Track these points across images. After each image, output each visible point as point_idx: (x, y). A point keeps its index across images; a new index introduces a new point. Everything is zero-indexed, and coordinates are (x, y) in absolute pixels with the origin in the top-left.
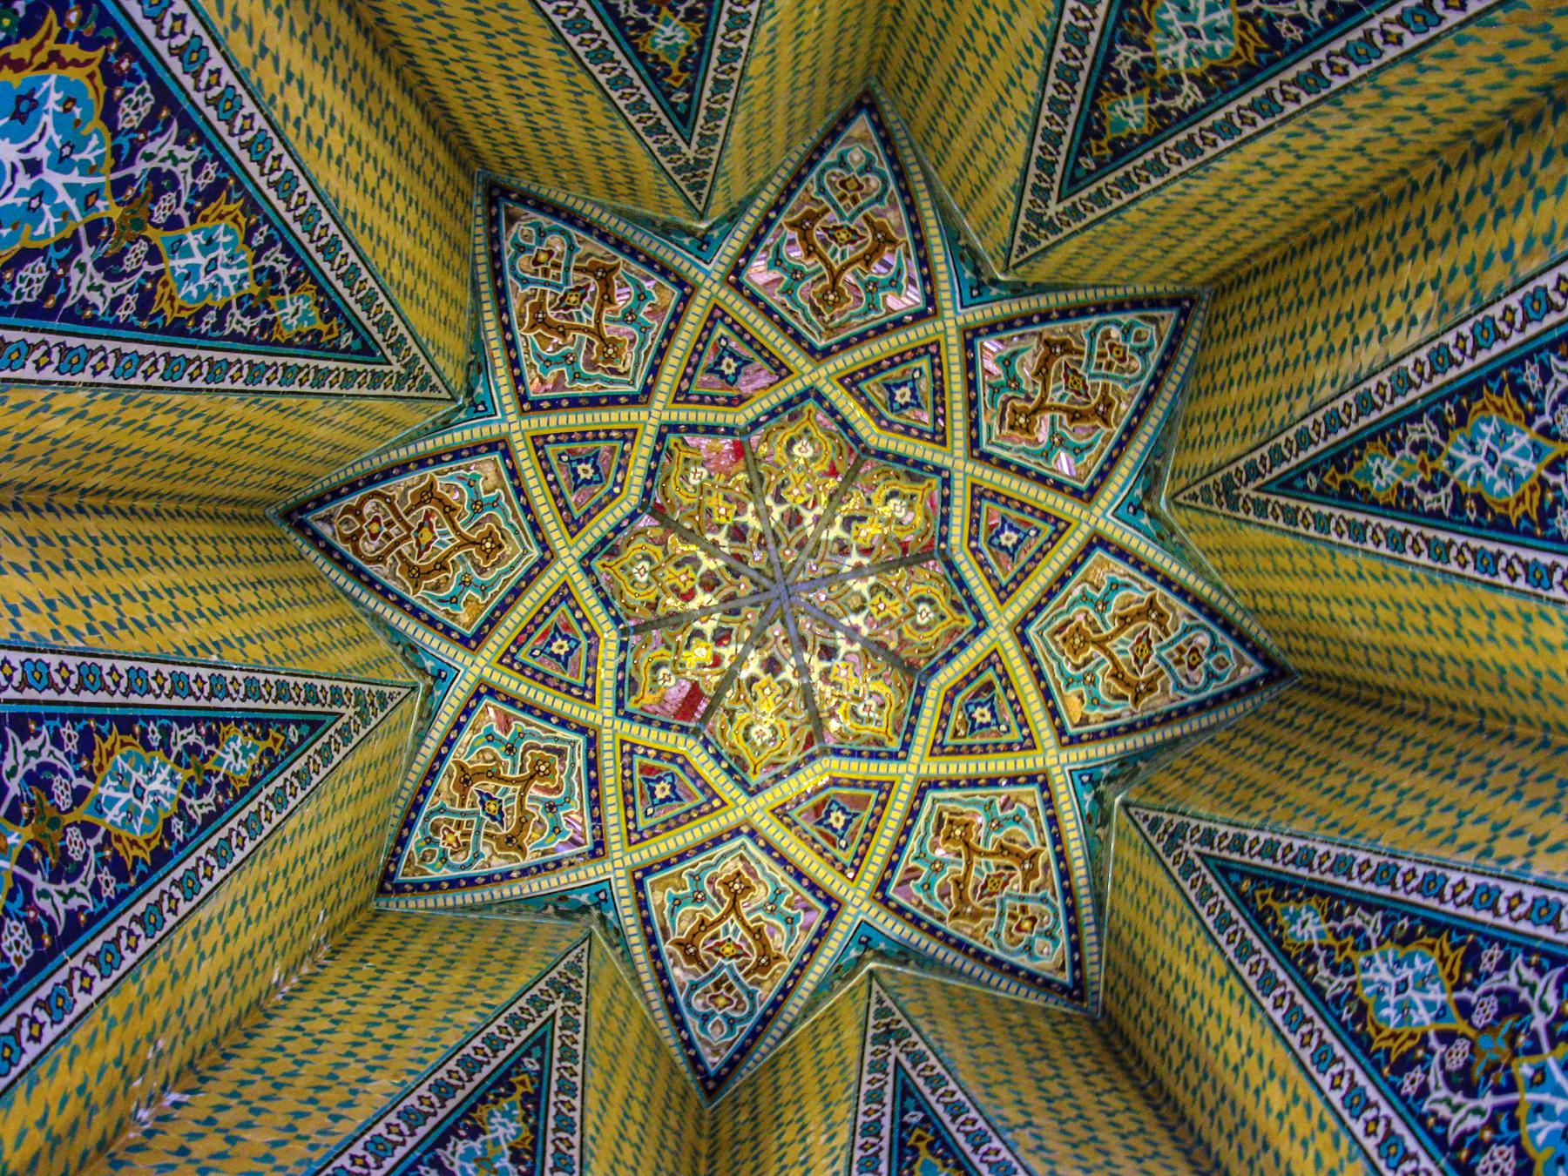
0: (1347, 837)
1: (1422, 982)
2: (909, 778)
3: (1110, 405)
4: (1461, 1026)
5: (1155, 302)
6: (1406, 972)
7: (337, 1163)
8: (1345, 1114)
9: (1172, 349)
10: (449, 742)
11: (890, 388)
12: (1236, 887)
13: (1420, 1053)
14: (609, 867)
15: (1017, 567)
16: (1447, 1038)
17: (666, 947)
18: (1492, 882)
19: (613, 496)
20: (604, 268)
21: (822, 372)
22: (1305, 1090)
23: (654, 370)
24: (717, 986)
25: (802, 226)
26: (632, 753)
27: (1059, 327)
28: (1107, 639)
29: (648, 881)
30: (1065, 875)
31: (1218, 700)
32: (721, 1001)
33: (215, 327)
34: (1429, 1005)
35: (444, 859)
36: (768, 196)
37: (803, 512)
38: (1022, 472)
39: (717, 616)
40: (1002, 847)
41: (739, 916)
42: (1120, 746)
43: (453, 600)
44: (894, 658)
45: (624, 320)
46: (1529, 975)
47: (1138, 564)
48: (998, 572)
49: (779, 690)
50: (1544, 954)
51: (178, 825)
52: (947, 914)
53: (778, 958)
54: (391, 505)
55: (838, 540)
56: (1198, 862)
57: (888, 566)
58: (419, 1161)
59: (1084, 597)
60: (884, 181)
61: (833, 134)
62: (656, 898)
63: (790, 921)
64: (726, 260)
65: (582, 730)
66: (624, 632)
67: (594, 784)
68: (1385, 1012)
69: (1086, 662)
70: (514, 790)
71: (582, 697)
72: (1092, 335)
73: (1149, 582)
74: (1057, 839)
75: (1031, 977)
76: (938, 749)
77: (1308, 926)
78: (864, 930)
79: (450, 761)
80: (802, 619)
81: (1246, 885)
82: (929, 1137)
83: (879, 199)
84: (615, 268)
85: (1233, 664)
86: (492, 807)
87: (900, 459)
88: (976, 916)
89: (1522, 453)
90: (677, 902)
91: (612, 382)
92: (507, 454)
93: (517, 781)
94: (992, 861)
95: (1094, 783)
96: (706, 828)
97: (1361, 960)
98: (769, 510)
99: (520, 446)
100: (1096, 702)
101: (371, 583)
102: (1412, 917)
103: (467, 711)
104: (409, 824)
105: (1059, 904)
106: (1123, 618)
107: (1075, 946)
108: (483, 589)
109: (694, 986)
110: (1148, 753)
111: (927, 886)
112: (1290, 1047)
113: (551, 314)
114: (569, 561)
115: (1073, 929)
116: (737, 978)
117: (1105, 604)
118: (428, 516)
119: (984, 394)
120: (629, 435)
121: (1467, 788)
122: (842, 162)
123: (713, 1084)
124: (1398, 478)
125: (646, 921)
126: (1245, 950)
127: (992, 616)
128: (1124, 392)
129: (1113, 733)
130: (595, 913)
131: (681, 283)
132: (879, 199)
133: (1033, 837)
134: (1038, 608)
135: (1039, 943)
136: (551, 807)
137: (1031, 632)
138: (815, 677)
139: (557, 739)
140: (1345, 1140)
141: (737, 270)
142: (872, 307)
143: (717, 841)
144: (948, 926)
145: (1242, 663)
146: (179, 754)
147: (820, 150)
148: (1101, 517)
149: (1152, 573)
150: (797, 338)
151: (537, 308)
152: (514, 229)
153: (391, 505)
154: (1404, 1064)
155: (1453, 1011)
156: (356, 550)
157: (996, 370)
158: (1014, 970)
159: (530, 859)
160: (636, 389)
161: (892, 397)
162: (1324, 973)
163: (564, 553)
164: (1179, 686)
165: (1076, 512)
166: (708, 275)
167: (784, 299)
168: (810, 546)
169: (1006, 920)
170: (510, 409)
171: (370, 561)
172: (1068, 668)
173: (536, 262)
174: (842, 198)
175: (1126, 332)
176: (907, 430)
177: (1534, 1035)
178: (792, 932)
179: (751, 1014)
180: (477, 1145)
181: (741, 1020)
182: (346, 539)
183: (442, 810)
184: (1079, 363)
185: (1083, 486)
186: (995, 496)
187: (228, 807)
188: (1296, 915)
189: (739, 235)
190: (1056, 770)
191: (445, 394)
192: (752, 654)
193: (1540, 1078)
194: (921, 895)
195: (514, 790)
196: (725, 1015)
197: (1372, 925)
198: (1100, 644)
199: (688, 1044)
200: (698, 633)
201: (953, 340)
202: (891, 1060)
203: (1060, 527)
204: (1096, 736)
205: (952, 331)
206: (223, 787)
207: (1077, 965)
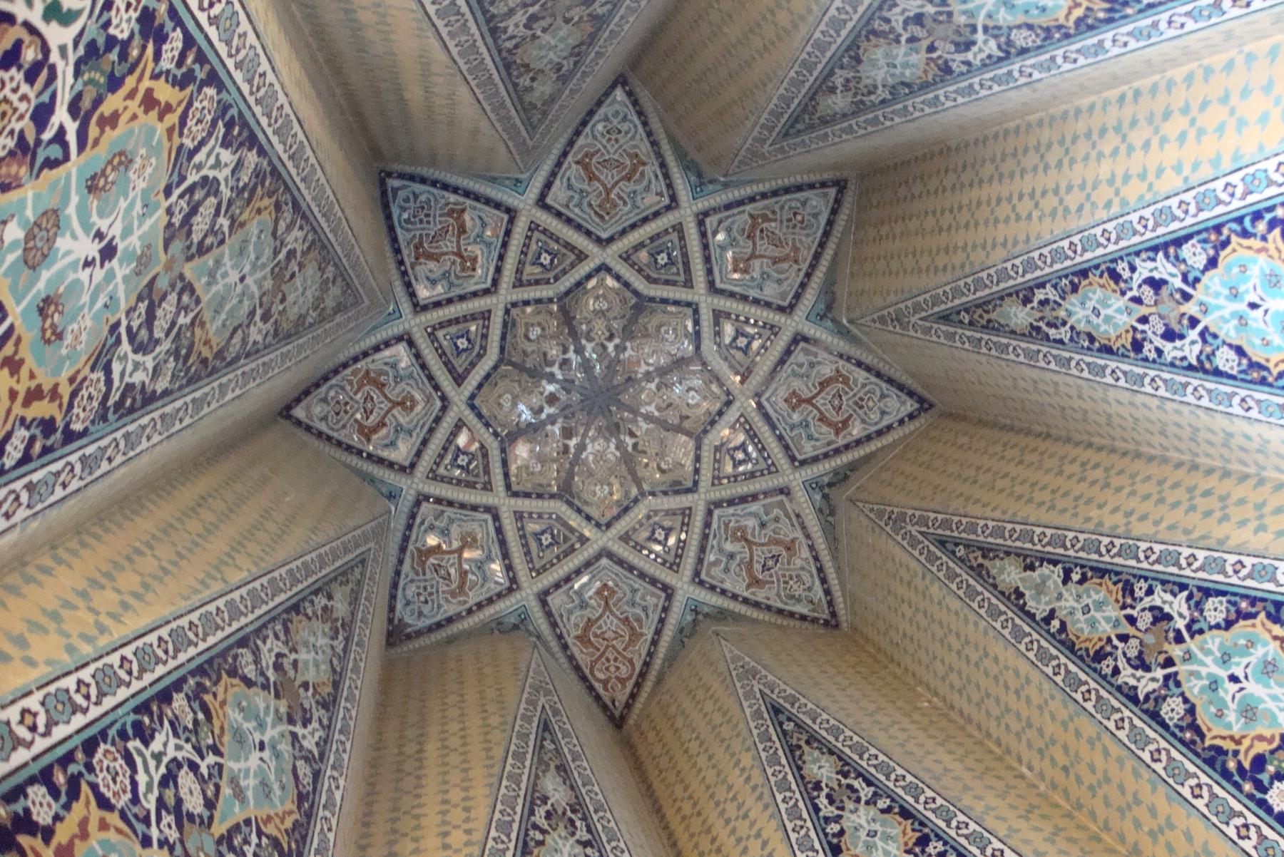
2: (709, 300)
3: (453, 211)
5: (384, 193)
7: (1061, 684)
9: (412, 178)
10: (735, 597)
11: (459, 352)
12: (799, 131)
13: (940, 62)
14: (794, 483)
15: (564, 251)
17: (841, 442)
19: (559, 519)
20: (419, 558)
21: (456, 399)
23: (475, 508)
24: (861, 407)
25: (367, 433)
26: (719, 478)
27: (405, 252)
28: (604, 185)
29: (799, 457)
30: (764, 196)
31: (640, 114)
32: (871, 404)
33: (592, 847)
35: (809, 589)
36: (354, 460)
37: (546, 394)
38: (501, 258)
39: (622, 437)
40: (748, 237)
41: (814, 397)
42: (675, 170)
43: (645, 609)
44: (633, 320)
45: (448, 535)
47: (553, 174)
48: (568, 262)
49: (664, 390)
51: (883, 803)
52: (796, 267)
53: (838, 371)
54: (596, 662)
55: (560, 368)
57: (574, 334)
58: (1048, 632)
59: (579, 205)
60: (331, 387)
61: (308, 429)
62: (808, 450)
63: (812, 365)
64: (398, 478)
65: (710, 513)
66: (643, 494)
67: (743, 499)
69: (620, 198)
70: (757, 551)
71: (690, 516)
72: (408, 230)
73: (565, 166)
74: (740, 203)
75: (834, 212)
76: (689, 284)
78: (812, 317)
79: (746, 594)
80: (615, 382)
81: (800, 126)
82: (980, 311)
83: (343, 388)
84: (418, 549)
85: (617, 107)
86: (770, 563)
87: (503, 337)
88: (796, 250)
90: (810, 437)
91: (488, 534)
92: (546, 593)
93: (750, 549)
94: (759, 243)
95: (701, 184)
96: (760, 424)
98: (549, 416)
99: (540, 585)
100: (647, 189)
101: (647, 664)
103: (713, 588)
104: (792, 615)
105: (784, 198)
106: (590, 179)
107: (811, 186)
108: (634, 591)
109: (863, 421)
110: (681, 155)
113: (454, 586)
114: (605, 539)
115: (799, 188)
116: (855, 395)
117: (582, 191)
118: (596, 636)
119: (457, 292)
120: (519, 516)
122: (325, 418)
123: (924, 405)
125: (826, 456)
126: (849, 130)
127: (597, 262)
128: (443, 201)
129: (667, 176)
130: (826, 490)
131: (418, 503)
132: (343, 388)
133: (741, 218)
134: (588, 233)
135: (808, 210)
136: (763, 525)
137: (604, 235)
138: (651, 369)
139: (719, 527)
141: (403, 469)
142: (411, 376)
143: (766, 417)
144: (805, 267)
145: (614, 101)
146: (838, 808)
147: (320, 434)
148: (525, 202)
149: (559, 164)
150: (438, 420)
151: (453, 594)
152: (410, 622)
153: (596, 662)
156: (629, 678)
157: (439, 289)
158: (830, 223)
159: (799, 534)
160: (488, 517)
161: (465, 350)
162: (873, 97)
163: (601, 543)
164: (633, 138)
165: (523, 219)
166: (410, 487)
167: (414, 434)
168: (566, 385)
169: (797, 230)
170: (518, 596)
171: (634, 669)
172: (627, 209)
173: (426, 602)
174: (346, 412)
175: (403, 209)
176: (485, 336)
178: (819, 363)
179: (877, 385)
180: (1027, 593)
181: (881, 389)
182: (624, 686)
183: (778, 595)
184: (427, 235)
185: (506, 217)
186: (519, 271)
187: (855, 769)
188: (828, 106)
189: (381, 473)
190: (694, 208)
191: (536, 655)
192: (643, 410)
195: (757, 551)
198: (608, 192)
199: (901, 422)
200: (635, 446)
201: (423, 318)
202: (920, 323)
203: (533, 227)
204: (670, 186)
205: (418, 320)
206: (846, 775)
207: (824, 185)
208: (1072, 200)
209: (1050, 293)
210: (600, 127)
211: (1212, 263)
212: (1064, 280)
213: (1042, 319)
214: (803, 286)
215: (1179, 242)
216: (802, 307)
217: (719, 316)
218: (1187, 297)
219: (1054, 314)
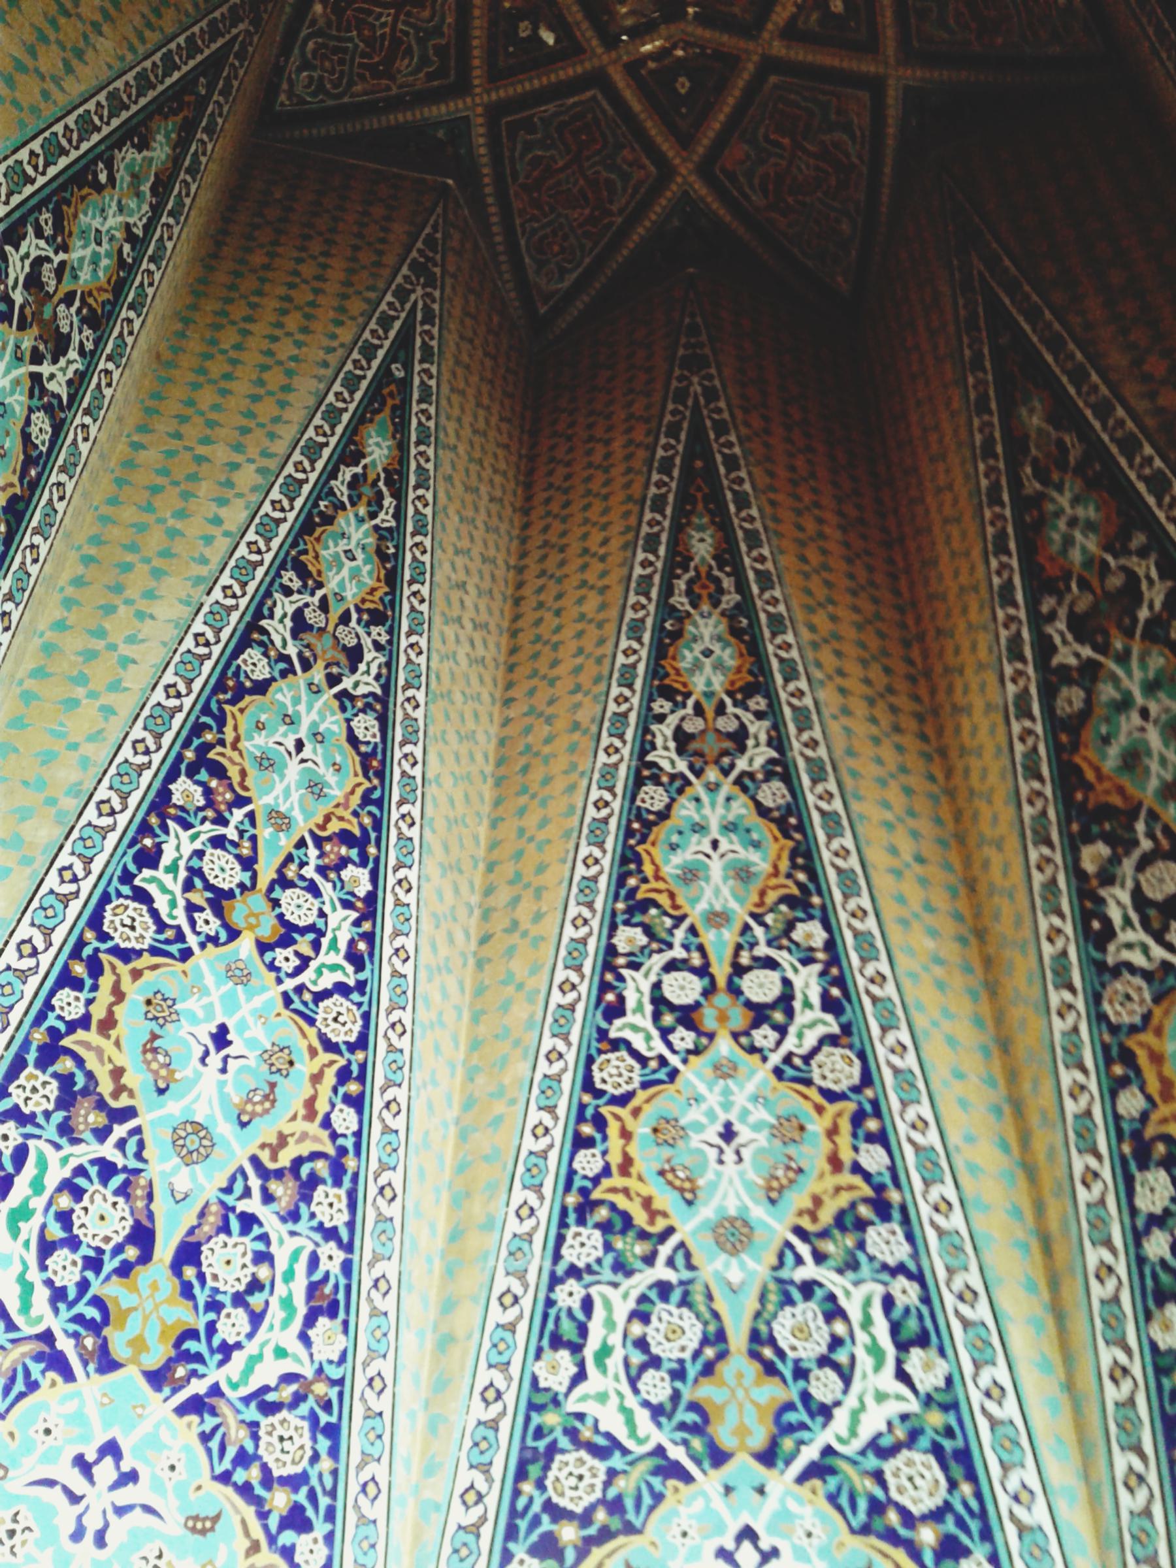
0: (771, 524)
1: (718, 666)
4: (710, 712)
6: (716, 648)
8: (616, 675)
16: (699, 710)
18: (801, 668)
22: (611, 628)
24: (336, 51)
34: (709, 683)
46: (763, 737)
50: (779, 738)
53: (392, 78)
56: (690, 402)
63: (424, 61)
68: (687, 653)
77: (702, 547)
81: (699, 464)
89: (1084, 550)
97: (705, 608)
102: (751, 625)
111: (528, 146)
112: (626, 598)
116: (352, 60)
121: (848, 583)
124: (1033, 435)
140: (602, 687)
154: (668, 693)
155: (715, 701)
158: (518, 266)
177: (732, 766)
181: (327, 93)
193: (713, 788)
194: (519, 147)
196: (321, 78)
197: (731, 599)
199: (278, 70)
208: (450, 631)
209: (385, 519)
210: (845, 227)
211: (353, 739)
212: (392, 551)
213: (365, 475)
214: (496, 159)
215: (384, 721)
216: (482, 130)
217: (570, 48)
218: (333, 680)
219: (365, 500)
